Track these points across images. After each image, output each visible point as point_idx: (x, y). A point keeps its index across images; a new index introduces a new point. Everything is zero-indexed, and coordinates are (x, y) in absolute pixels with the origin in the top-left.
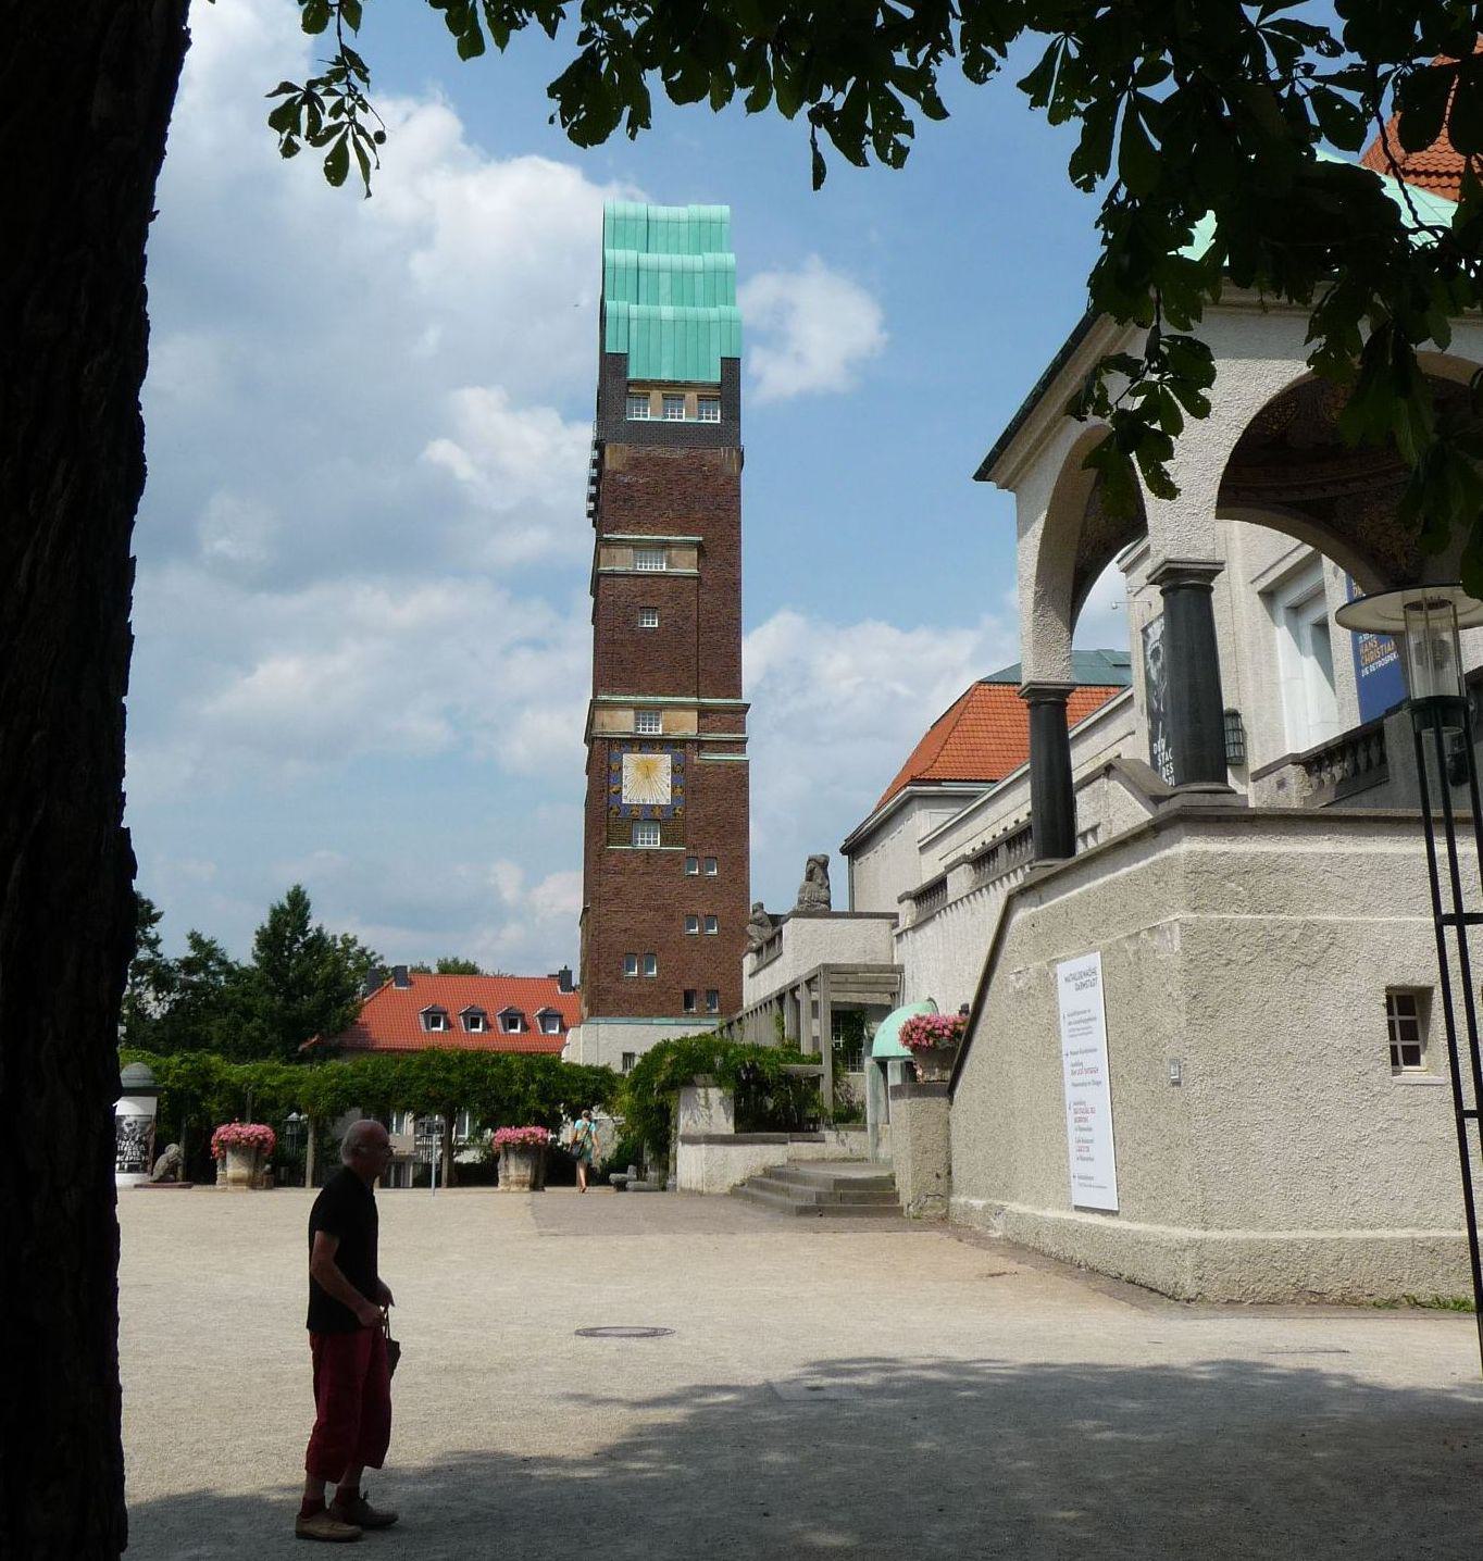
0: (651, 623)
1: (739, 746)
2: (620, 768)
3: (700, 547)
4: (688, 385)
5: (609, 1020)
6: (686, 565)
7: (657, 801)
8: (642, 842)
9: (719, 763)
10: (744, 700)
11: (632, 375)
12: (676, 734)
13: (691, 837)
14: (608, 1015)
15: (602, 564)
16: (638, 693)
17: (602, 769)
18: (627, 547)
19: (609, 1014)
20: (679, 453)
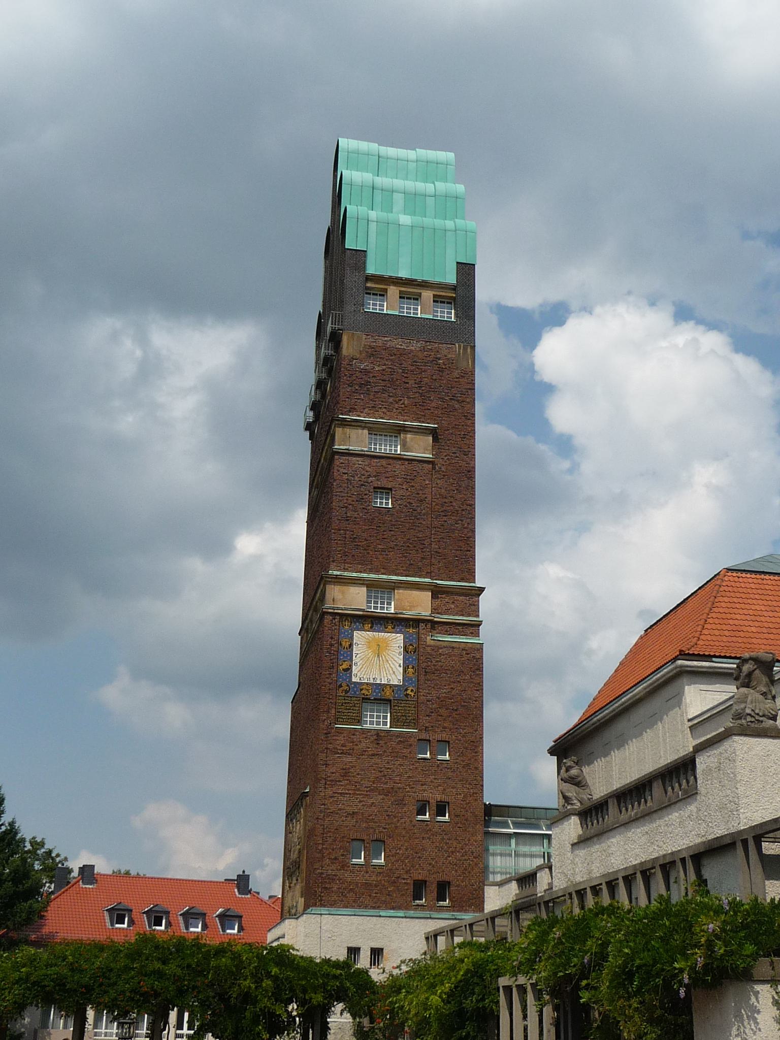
0: (385, 503)
1: (471, 629)
2: (351, 646)
3: (434, 433)
4: (425, 285)
5: (333, 910)
6: (420, 448)
7: (389, 680)
8: (372, 723)
10: (478, 584)
11: (371, 270)
12: (409, 614)
13: (424, 720)
14: (332, 906)
15: (336, 443)
16: (371, 571)
17: (331, 645)
18: (364, 428)
19: (332, 905)
20: (415, 346)
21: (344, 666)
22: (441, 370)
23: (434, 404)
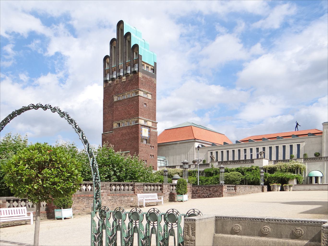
6: (150, 97)
22: (152, 83)
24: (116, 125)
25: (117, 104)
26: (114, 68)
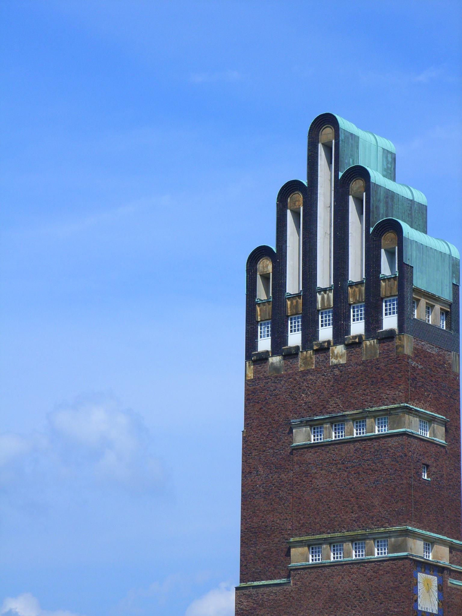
3: (445, 424)
4: (437, 299)
9: (459, 587)
21: (415, 598)
22: (446, 372)
23: (443, 401)
24: (302, 554)
25: (309, 456)
26: (292, 303)
